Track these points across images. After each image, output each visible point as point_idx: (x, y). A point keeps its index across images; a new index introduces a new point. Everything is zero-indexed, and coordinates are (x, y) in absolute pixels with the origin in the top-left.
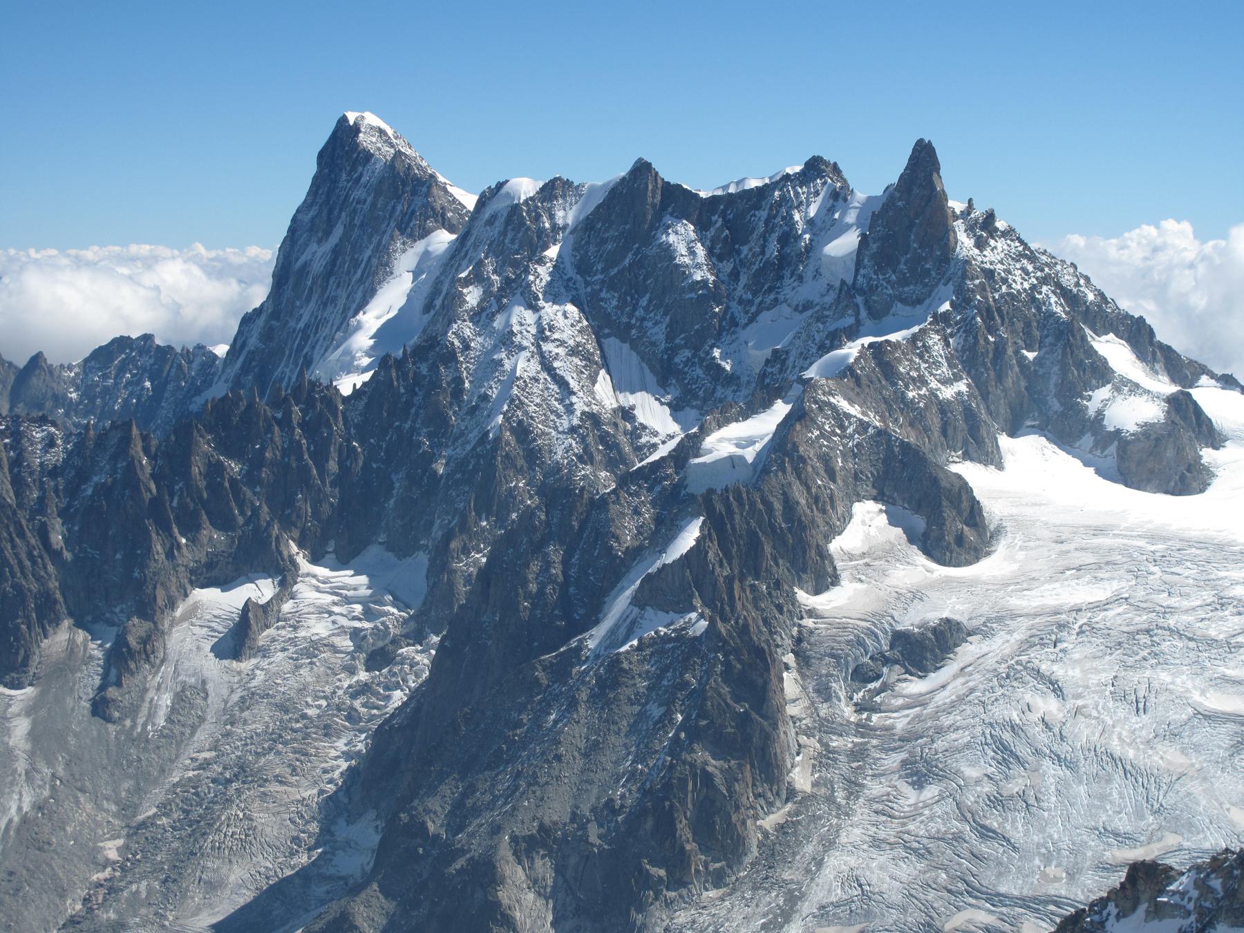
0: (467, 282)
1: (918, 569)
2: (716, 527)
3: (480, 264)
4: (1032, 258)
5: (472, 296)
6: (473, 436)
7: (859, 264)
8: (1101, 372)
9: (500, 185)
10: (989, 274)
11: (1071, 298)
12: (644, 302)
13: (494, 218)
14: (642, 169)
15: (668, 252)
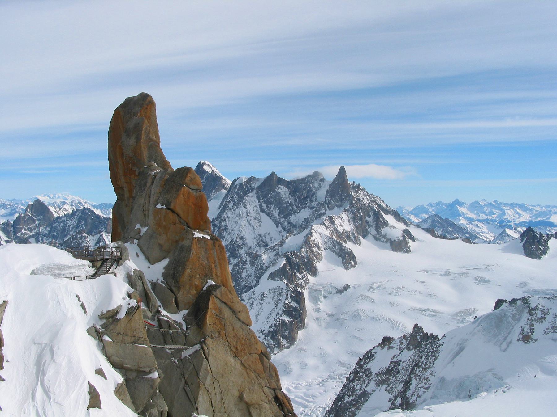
0: (229, 202)
1: (341, 270)
2: (288, 260)
3: (233, 197)
4: (369, 196)
5: (231, 205)
6: (230, 240)
7: (326, 197)
8: (386, 224)
9: (238, 178)
10: (359, 199)
11: (379, 206)
12: (273, 207)
13: (236, 186)
14: (273, 174)
15: (279, 194)
